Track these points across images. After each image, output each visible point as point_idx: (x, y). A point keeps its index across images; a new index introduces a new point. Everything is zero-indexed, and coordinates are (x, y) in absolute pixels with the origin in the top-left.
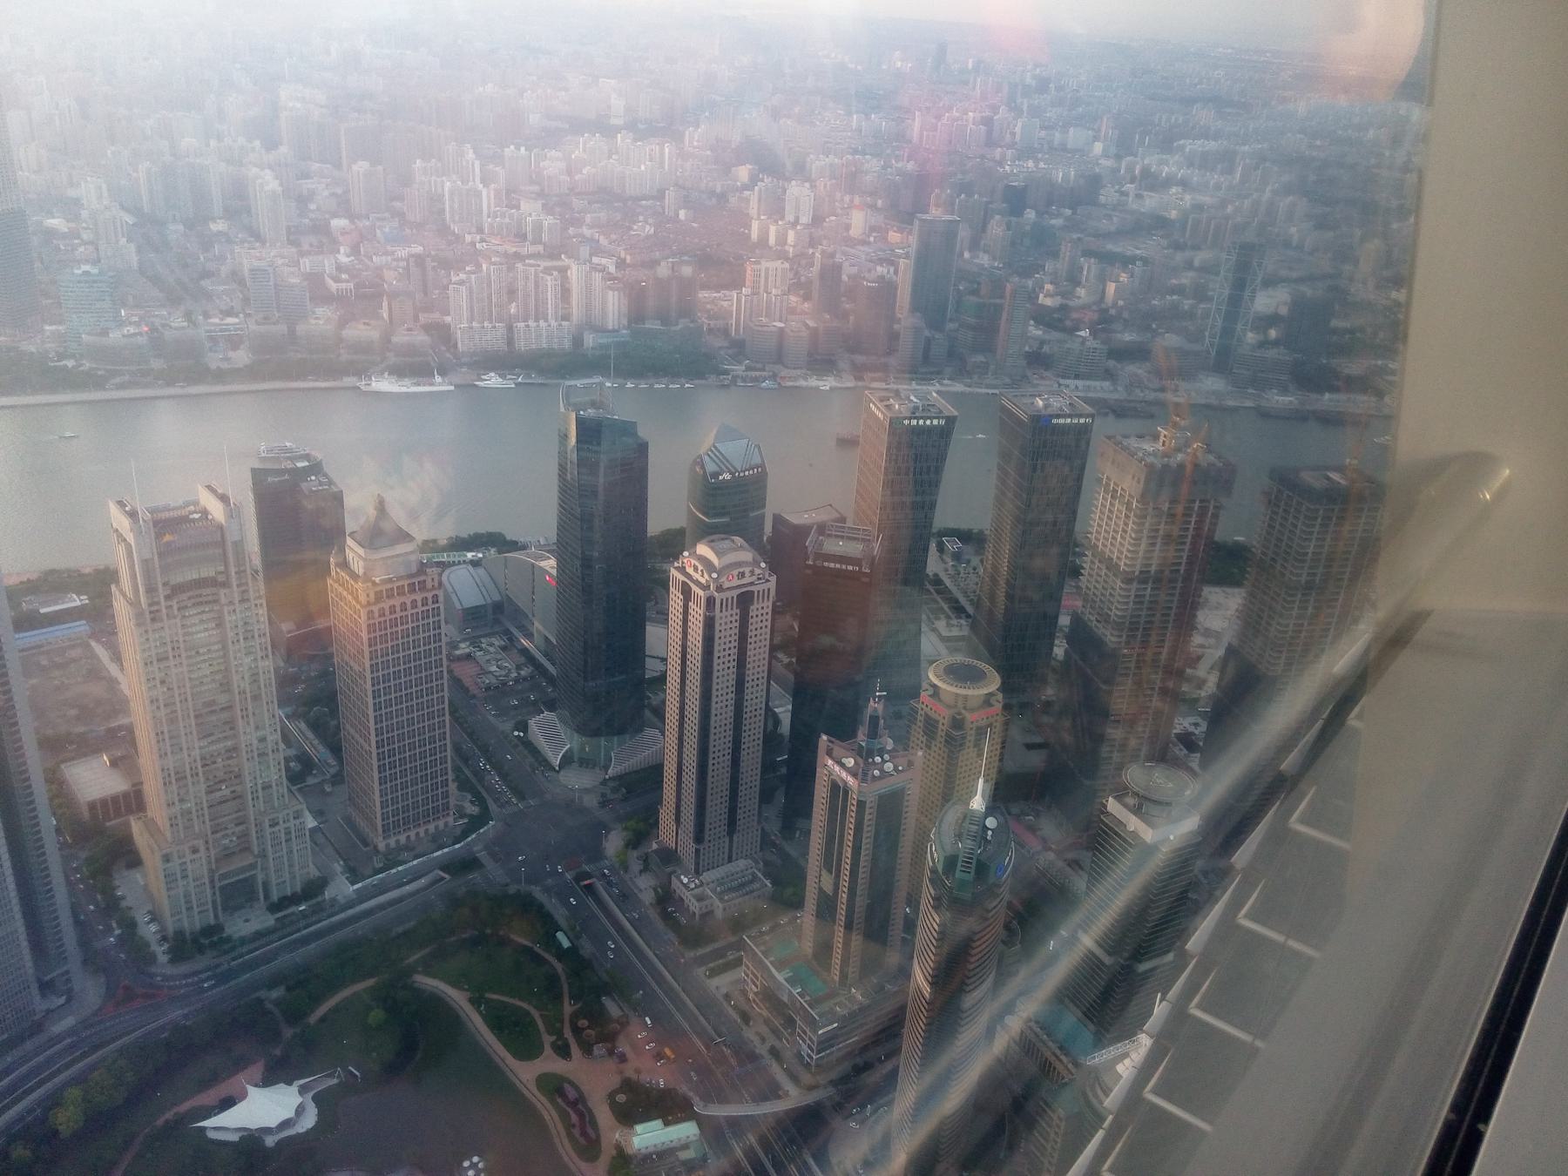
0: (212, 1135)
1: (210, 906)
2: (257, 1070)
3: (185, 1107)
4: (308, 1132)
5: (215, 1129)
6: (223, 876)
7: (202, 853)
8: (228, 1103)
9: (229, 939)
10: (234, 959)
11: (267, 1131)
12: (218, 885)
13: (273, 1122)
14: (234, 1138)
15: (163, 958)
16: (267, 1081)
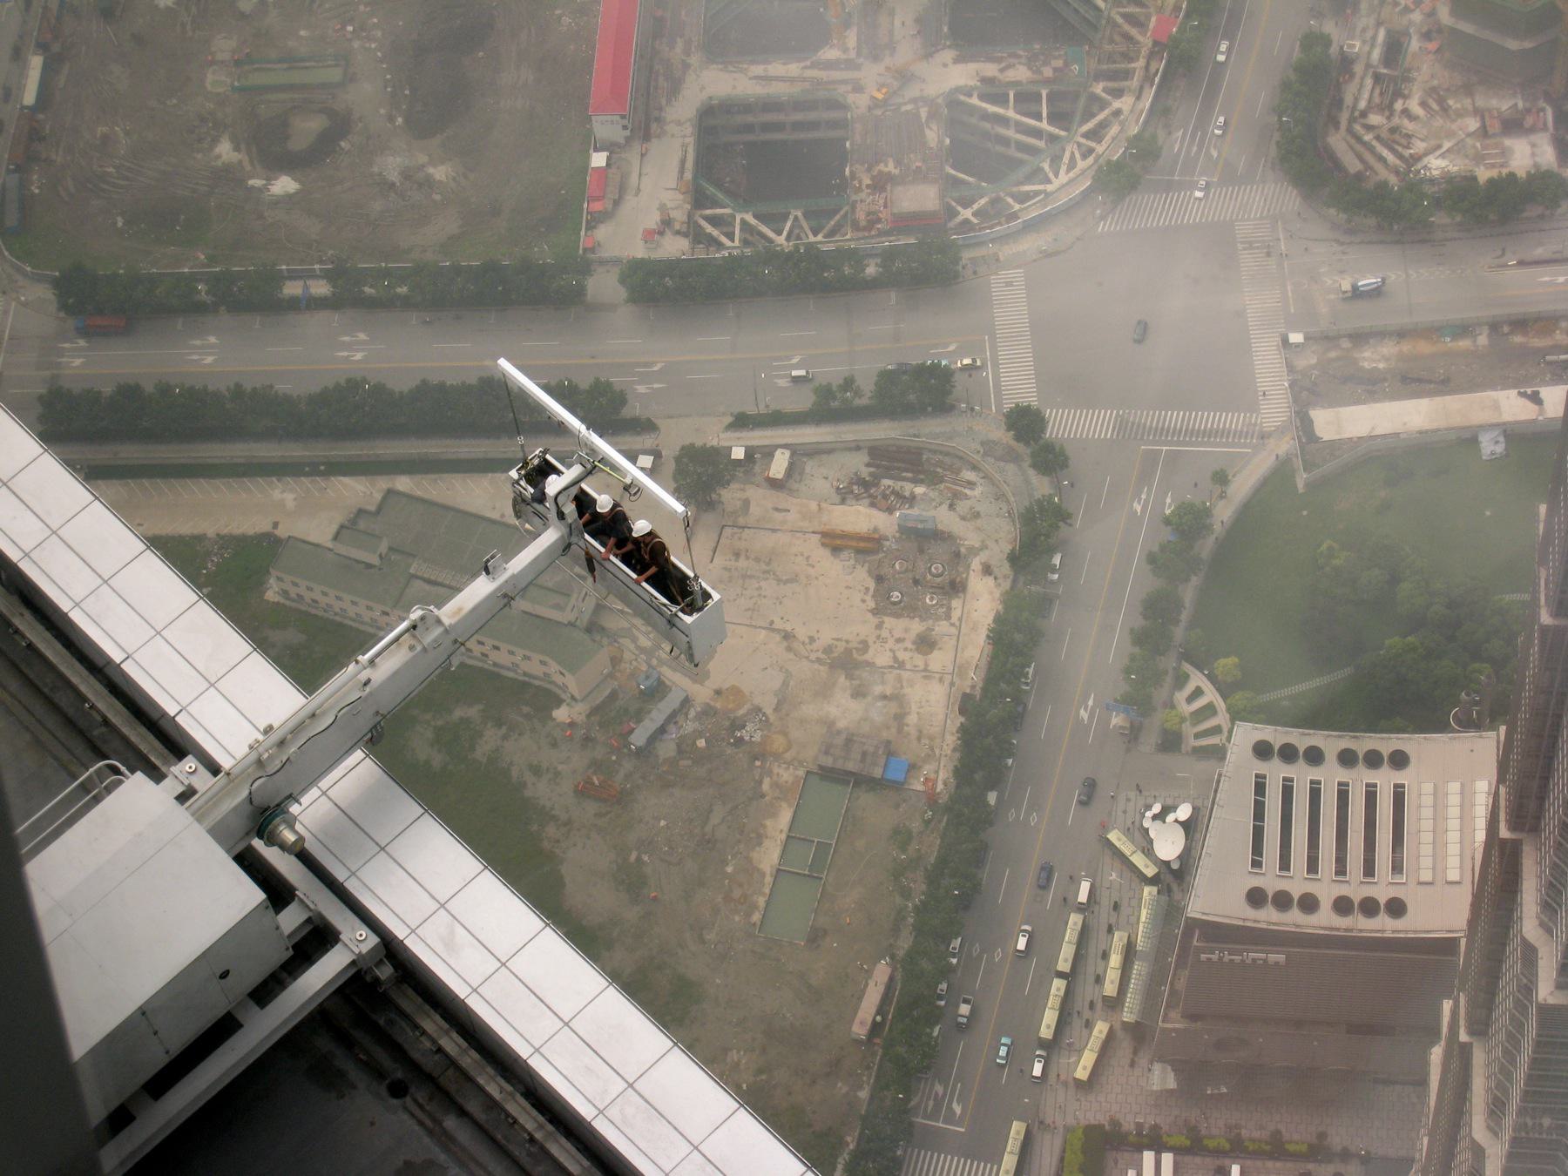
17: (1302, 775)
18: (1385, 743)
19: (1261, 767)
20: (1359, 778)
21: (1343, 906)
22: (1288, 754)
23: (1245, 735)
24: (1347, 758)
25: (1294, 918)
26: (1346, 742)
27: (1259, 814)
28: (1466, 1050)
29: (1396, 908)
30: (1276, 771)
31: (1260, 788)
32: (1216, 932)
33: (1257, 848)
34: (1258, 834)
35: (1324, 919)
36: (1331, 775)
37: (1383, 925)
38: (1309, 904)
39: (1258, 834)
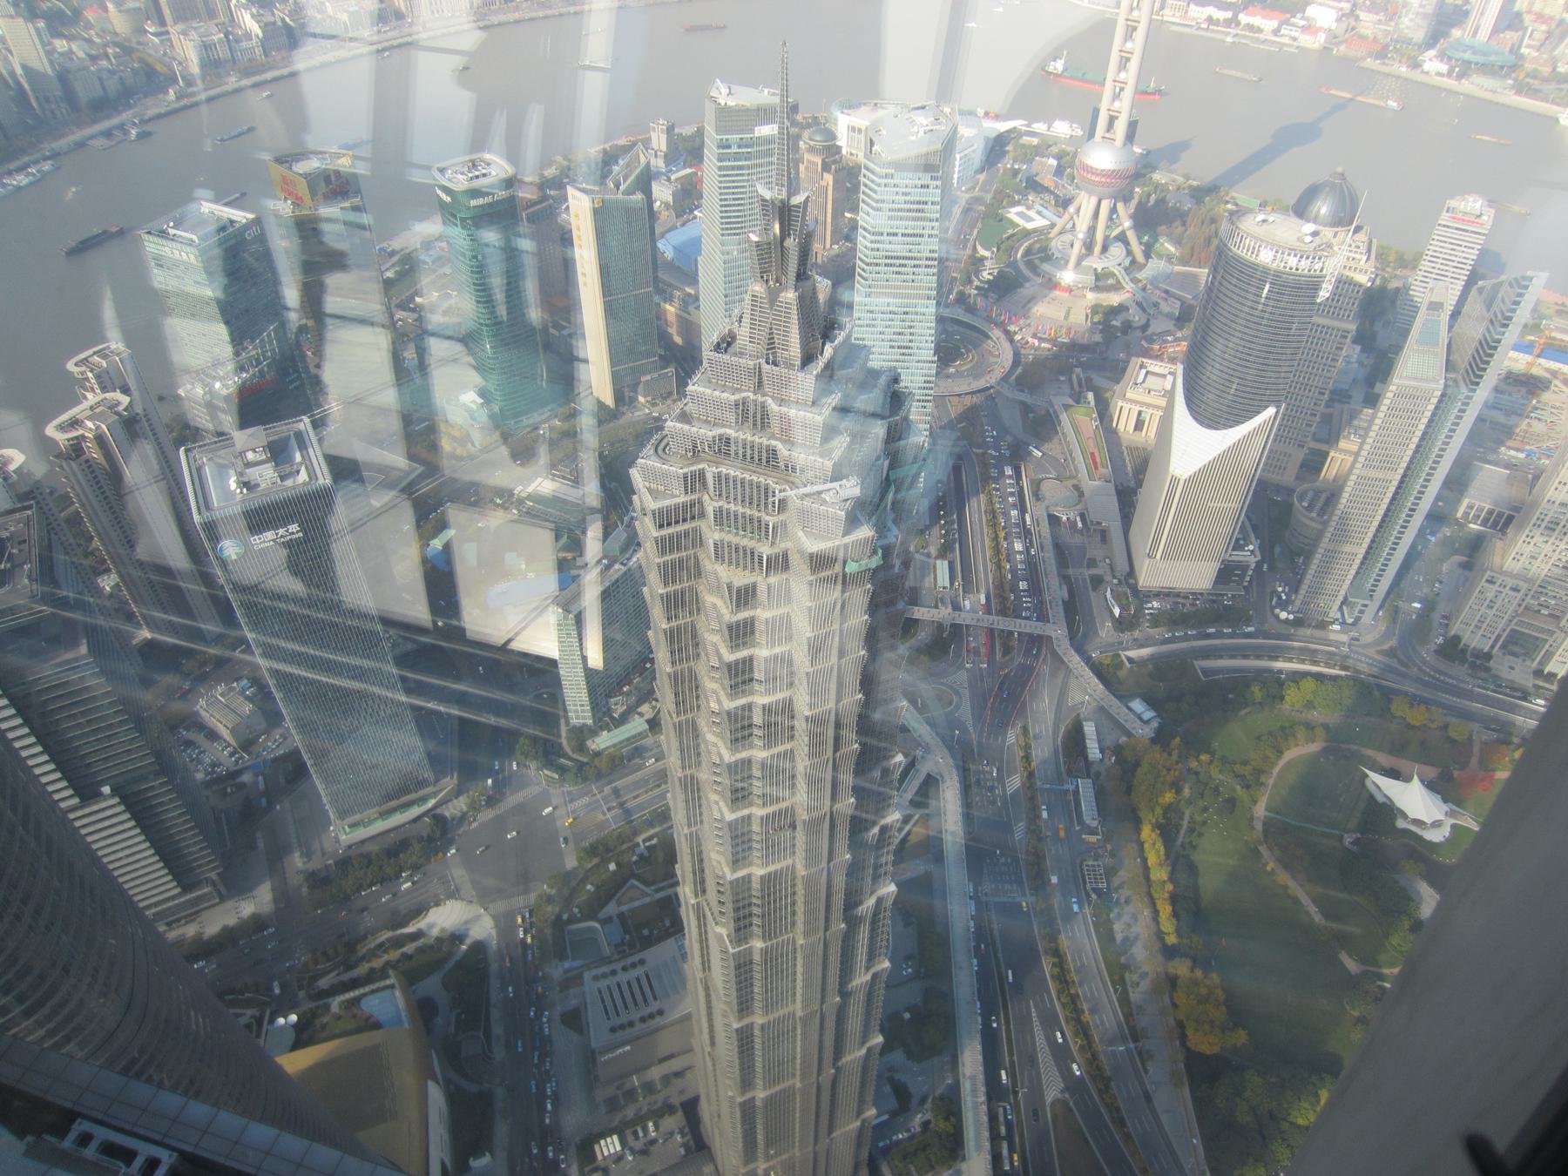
0: (1368, 783)
1: (1494, 637)
2: (1432, 772)
3: (1370, 752)
4: (1430, 843)
5: (1374, 783)
6: (1521, 623)
7: (1519, 595)
8: (1394, 774)
9: (1488, 670)
10: (1479, 687)
11: (1405, 816)
12: (1512, 626)
13: (1412, 814)
14: (1380, 799)
15: (1433, 647)
16: (1431, 786)
18: (636, 958)
24: (625, 969)
26: (622, 964)
31: (600, 992)
33: (607, 1013)
34: (605, 1007)
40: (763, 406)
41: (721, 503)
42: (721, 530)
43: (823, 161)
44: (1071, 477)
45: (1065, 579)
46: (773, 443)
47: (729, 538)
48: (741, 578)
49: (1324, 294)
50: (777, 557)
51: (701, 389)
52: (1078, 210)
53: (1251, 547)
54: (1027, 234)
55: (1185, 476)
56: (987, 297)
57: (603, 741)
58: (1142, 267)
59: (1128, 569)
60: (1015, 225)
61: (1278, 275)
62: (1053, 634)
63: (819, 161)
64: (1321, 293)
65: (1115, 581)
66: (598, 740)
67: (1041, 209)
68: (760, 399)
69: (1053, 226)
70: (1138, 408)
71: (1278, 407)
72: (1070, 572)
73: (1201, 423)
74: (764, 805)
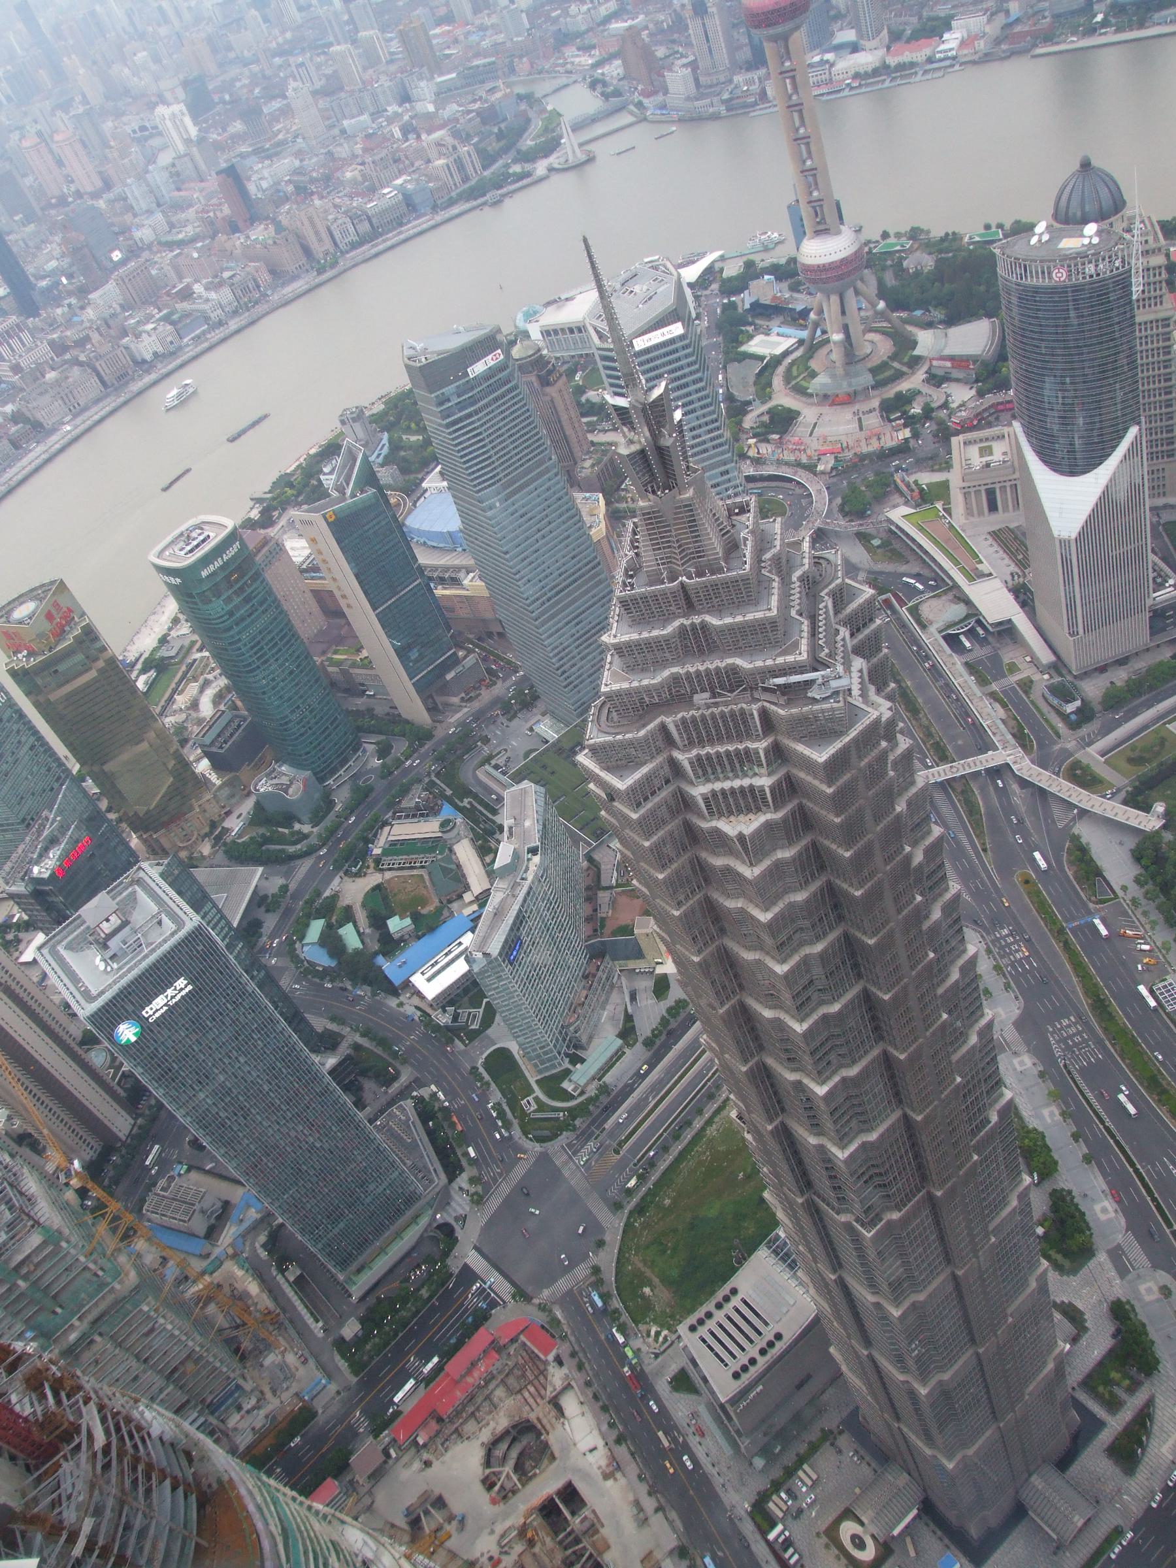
17: (711, 1324)
18: (725, 1290)
19: (697, 1335)
20: (728, 1308)
21: (763, 1352)
22: (701, 1322)
23: (682, 1329)
24: (719, 1306)
25: (753, 1371)
27: (712, 1349)
28: (871, 1357)
29: (778, 1336)
30: (703, 1331)
31: (704, 1341)
32: (734, 1401)
33: (722, 1361)
34: (717, 1355)
35: (762, 1362)
36: (719, 1316)
37: (780, 1346)
38: (753, 1361)
39: (717, 1355)
40: (704, 626)
41: (694, 752)
42: (708, 781)
43: (539, 377)
44: (950, 589)
45: (993, 696)
46: (730, 661)
47: (718, 786)
48: (747, 825)
49: (1136, 290)
50: (779, 783)
51: (625, 638)
52: (820, 312)
53: (1171, 582)
54: (776, 361)
55: (1074, 535)
56: (768, 441)
57: (581, 1075)
58: (914, 344)
59: (1052, 658)
60: (762, 358)
61: (1077, 289)
62: (1009, 760)
63: (533, 379)
64: (1134, 289)
65: (1046, 677)
66: (574, 1077)
67: (782, 330)
68: (697, 619)
69: (801, 342)
70: (983, 488)
71: (1139, 423)
72: (995, 687)
73: (1062, 473)
74: (854, 1062)
